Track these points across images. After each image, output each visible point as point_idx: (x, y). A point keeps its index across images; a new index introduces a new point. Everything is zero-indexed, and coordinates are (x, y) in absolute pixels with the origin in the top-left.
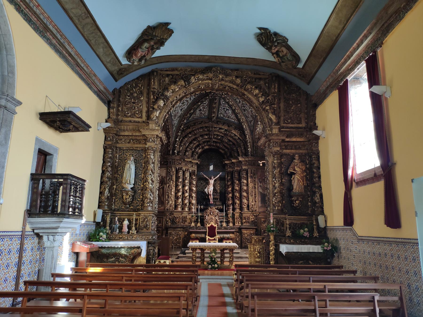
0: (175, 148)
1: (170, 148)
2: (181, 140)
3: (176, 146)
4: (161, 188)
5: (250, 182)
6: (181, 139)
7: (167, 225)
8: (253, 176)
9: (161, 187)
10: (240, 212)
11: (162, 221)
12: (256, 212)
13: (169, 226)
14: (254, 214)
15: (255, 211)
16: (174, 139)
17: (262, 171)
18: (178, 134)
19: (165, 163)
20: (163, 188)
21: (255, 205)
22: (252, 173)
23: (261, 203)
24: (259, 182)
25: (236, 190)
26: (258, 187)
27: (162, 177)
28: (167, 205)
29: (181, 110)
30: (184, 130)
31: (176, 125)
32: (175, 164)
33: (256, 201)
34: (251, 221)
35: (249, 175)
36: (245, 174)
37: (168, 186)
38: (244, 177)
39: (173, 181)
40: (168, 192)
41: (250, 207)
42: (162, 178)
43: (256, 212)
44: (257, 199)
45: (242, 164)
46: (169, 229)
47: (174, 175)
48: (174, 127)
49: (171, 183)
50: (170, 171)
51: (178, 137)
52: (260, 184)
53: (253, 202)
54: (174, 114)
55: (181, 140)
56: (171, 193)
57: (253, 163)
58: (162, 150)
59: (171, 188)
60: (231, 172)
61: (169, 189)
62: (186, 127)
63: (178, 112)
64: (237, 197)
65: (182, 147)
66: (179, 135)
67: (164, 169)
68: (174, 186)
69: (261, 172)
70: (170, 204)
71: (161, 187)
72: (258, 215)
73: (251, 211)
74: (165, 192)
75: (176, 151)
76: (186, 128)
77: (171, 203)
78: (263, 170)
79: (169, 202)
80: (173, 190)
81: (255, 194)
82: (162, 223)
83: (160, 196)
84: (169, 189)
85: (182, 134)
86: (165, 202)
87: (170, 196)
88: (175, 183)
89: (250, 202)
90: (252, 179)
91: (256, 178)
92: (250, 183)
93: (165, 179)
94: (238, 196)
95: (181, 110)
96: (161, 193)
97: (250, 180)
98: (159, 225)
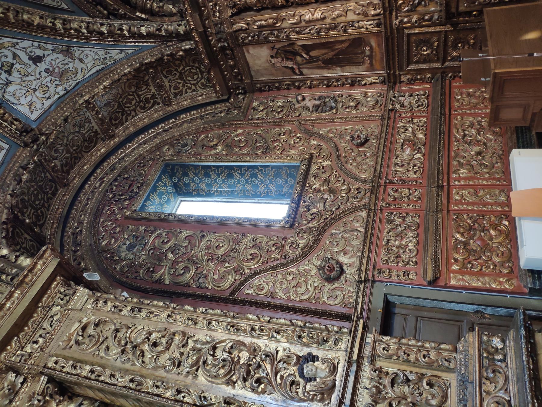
0: (172, 33)
1: (178, 51)
2: (143, 16)
3: (166, 30)
4: (307, 54)
6: (142, 12)
7: (436, 17)
9: (305, 56)
11: (421, 37)
13: (441, 11)
16: (147, 42)
18: (126, 33)
19: (227, 54)
20: (307, 48)
27: (272, 57)
28: (363, 27)
29: (36, 60)
30: (109, 13)
31: (101, 53)
32: (221, 24)
37: (298, 33)
39: (277, 19)
40: (318, 33)
42: (277, 58)
46: (453, 10)
47: (256, 18)
48: (108, 56)
49: (286, 24)
50: (248, 37)
51: (135, 34)
54: (57, 85)
55: (143, 16)
56: (317, 20)
58: (193, 71)
59: (301, 22)
61: (307, 30)
62: (99, 11)
63: (47, 71)
65: (163, 7)
66: (129, 31)
67: (246, 54)
68: (292, 13)
70: (355, 17)
71: (305, 56)
74: (318, 41)
75: (181, 29)
76: (99, 7)
77: (354, 13)
79: (351, 24)
80: (308, 17)
82: (428, 37)
83: (333, 53)
84: (307, 30)
85: (125, 14)
86: (352, 37)
87: (328, 21)
88: (284, 13)
93: (277, 46)
95: (36, 60)
96: (323, 51)
98: (436, 44)
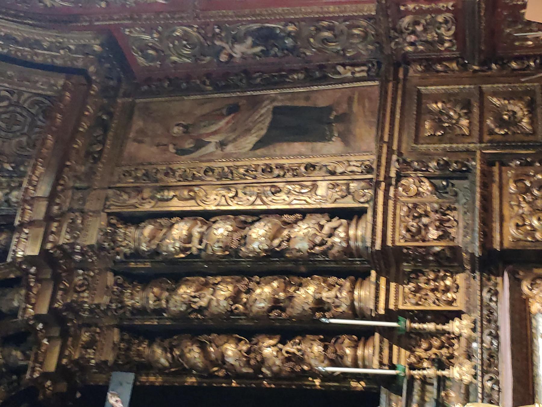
5: (192, 202)
8: (157, 181)
10: (373, 273)
12: (374, 166)
14: (393, 174)
15: (369, 170)
17: (135, 140)
21: (333, 173)
22: (139, 190)
23: (324, 138)
24: (194, 155)
25: (235, 298)
26: (227, 156)
33: (310, 167)
34: (435, 198)
35: (148, 207)
36: (132, 231)
38: (153, 237)
41: (349, 203)
43: (374, 166)
44: (299, 161)
45: (72, 245)
52: (211, 148)
53: (314, 187)
57: (77, 178)
60: (122, 340)
64: (275, 291)
69: (140, 142)
72: (400, 154)
73: (369, 192)
78: (132, 135)
81: (268, 170)
89: (313, 202)
90: (168, 188)
91: (175, 167)
92: (192, 198)
94: (275, 284)
97: (175, 202)
